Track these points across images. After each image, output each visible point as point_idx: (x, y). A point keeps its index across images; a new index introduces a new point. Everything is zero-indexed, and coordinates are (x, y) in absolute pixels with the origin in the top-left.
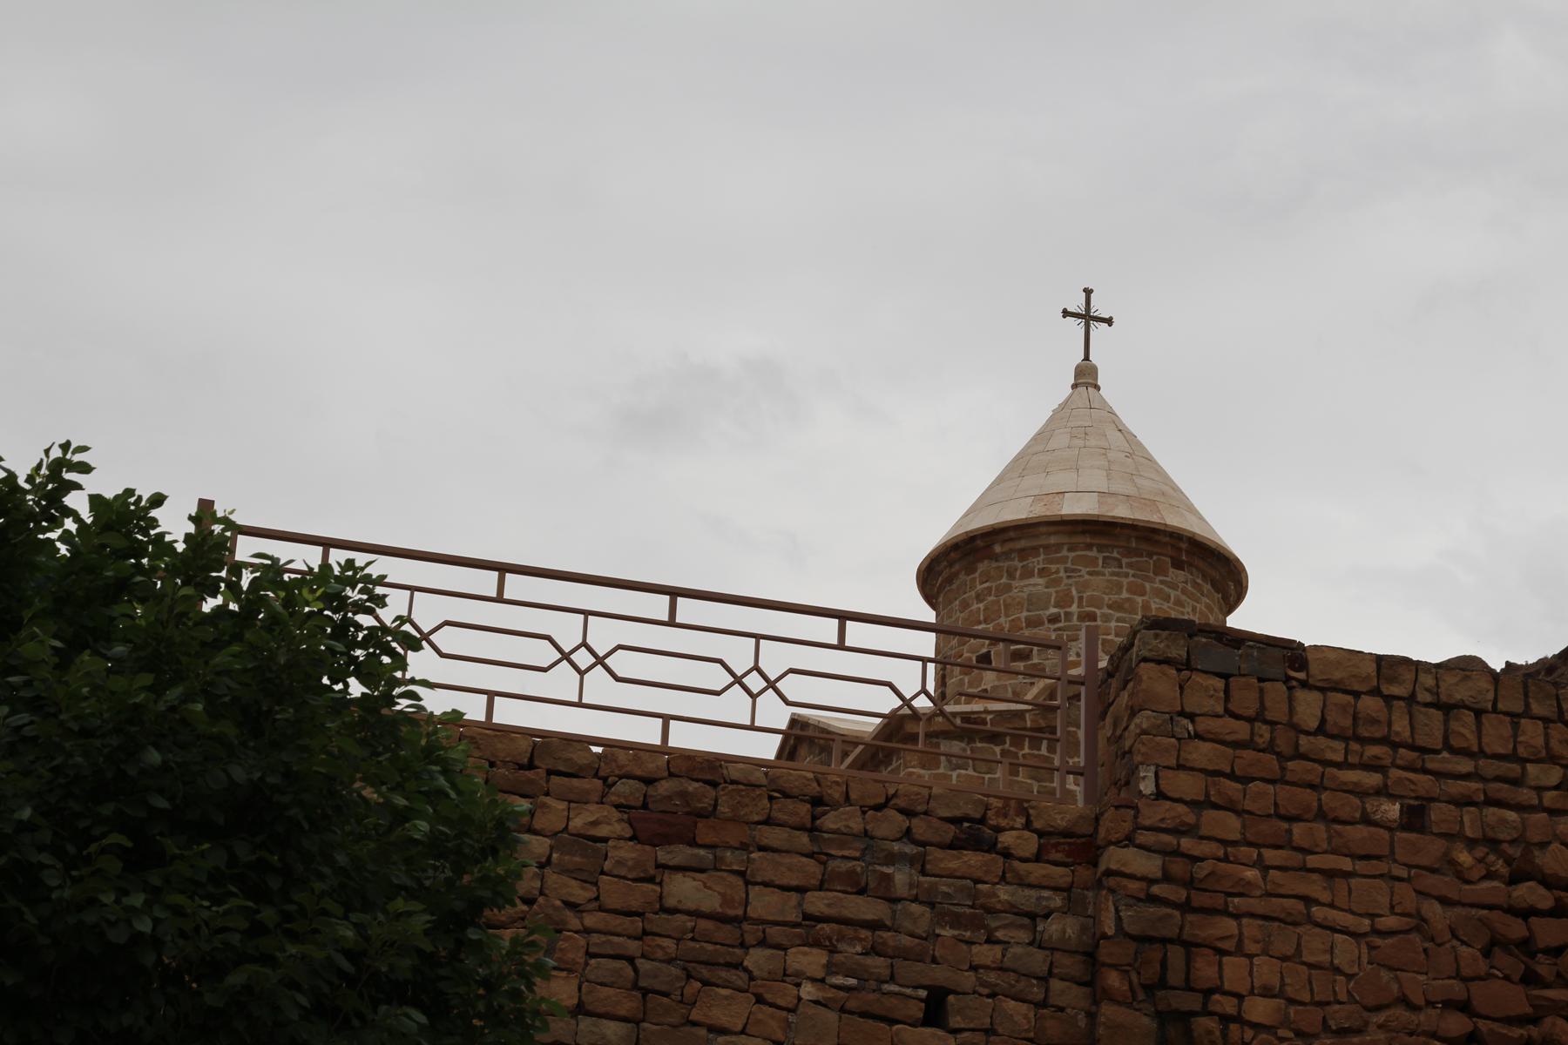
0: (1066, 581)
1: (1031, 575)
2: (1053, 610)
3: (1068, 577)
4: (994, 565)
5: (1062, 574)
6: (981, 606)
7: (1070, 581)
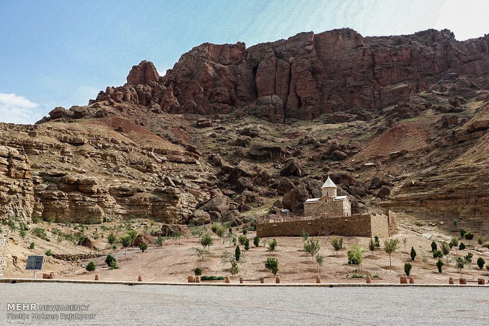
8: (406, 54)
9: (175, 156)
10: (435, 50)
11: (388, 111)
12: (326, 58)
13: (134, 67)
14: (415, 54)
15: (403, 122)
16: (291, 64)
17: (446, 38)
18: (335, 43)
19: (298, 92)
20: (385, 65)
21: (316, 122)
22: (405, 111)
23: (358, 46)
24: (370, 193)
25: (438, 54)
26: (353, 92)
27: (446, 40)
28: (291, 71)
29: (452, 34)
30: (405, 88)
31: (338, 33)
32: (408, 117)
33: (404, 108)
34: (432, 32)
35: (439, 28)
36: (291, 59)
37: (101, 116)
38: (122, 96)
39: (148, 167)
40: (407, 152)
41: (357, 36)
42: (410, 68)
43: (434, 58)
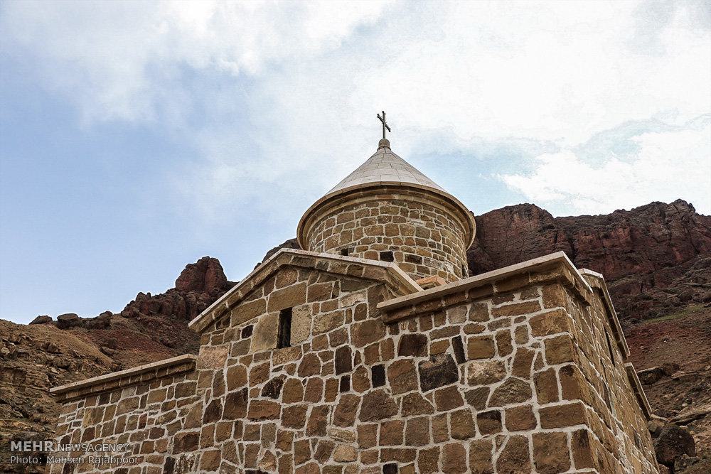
0: (436, 227)
1: (417, 217)
2: (430, 240)
3: (437, 226)
4: (391, 205)
5: (434, 222)
8: (623, 233)
12: (495, 250)
13: (189, 266)
14: (638, 234)
17: (682, 211)
18: (508, 226)
22: (644, 307)
23: (544, 228)
25: (676, 233)
27: (682, 214)
29: (691, 206)
30: (632, 283)
32: (652, 315)
33: (642, 302)
35: (668, 199)
40: (676, 368)
41: (543, 215)
42: (633, 255)
43: (670, 240)
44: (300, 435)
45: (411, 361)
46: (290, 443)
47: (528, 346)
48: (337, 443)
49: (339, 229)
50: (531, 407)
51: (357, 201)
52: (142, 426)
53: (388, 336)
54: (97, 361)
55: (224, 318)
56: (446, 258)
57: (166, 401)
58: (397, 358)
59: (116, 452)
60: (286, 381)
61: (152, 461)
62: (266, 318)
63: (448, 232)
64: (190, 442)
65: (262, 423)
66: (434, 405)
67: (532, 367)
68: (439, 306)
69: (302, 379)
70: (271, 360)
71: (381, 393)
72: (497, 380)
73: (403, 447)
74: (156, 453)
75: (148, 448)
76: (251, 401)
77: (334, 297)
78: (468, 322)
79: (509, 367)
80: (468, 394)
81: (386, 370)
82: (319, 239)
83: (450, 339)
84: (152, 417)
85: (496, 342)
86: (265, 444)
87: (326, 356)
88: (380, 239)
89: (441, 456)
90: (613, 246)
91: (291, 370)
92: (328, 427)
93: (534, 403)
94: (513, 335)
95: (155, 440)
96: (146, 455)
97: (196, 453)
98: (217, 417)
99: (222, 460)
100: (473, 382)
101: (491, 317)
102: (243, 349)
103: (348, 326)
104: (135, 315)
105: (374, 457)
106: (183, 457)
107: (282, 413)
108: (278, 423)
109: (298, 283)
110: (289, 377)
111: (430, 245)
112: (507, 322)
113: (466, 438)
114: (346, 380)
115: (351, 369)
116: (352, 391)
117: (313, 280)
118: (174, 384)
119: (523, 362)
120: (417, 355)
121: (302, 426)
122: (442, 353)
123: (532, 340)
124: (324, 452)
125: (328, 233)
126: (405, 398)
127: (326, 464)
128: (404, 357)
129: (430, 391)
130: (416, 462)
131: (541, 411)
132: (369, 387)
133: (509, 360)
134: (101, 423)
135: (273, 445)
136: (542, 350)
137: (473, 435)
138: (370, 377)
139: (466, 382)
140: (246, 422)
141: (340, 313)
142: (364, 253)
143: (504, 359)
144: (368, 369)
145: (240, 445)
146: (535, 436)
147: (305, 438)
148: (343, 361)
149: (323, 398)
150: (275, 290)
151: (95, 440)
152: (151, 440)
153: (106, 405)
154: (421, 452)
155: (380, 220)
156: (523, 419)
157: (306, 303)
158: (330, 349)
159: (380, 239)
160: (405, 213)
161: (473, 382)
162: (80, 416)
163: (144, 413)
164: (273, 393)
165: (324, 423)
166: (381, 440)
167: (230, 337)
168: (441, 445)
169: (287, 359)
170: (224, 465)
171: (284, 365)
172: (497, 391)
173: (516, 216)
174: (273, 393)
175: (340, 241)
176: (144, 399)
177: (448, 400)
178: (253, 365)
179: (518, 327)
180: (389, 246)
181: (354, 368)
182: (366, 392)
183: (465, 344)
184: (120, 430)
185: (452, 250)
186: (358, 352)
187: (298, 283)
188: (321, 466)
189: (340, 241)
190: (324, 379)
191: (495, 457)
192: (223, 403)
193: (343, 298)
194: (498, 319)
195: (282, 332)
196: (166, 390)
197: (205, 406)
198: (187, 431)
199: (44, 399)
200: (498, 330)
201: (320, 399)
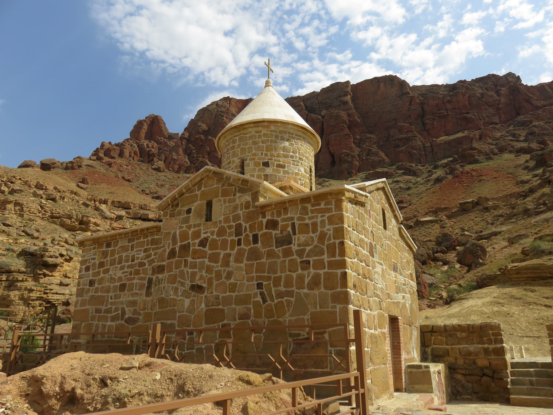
0: (295, 145)
2: (291, 154)
3: (296, 144)
5: (294, 142)
6: (264, 145)
7: (296, 146)
9: (142, 212)
10: (498, 95)
11: (443, 163)
15: (468, 168)
16: (323, 117)
17: (511, 82)
19: (331, 149)
20: (437, 113)
21: (351, 180)
24: (435, 260)
26: (398, 146)
28: (323, 125)
31: (378, 81)
32: (477, 162)
34: (492, 78)
35: (502, 72)
36: (323, 112)
37: (73, 168)
38: (118, 152)
39: (81, 222)
40: (487, 200)
41: (403, 84)
43: (499, 104)
44: (217, 267)
45: (271, 233)
46: (212, 271)
47: (325, 230)
48: (235, 272)
49: (239, 146)
50: (324, 259)
51: (250, 130)
52: (133, 260)
53: (260, 219)
54: (75, 193)
55: (176, 202)
56: (300, 164)
57: (146, 247)
58: (265, 231)
59: (119, 274)
60: (210, 239)
61: (141, 279)
62: (198, 204)
63: (303, 148)
64: (160, 269)
65: (198, 260)
66: (281, 255)
67: (326, 240)
68: (285, 206)
69: (218, 239)
70: (202, 228)
71: (256, 248)
72: (309, 245)
73: (266, 274)
74: (142, 275)
75: (137, 272)
76: (193, 249)
77: (234, 196)
78: (299, 215)
79: (316, 239)
80: (297, 251)
81: (259, 236)
82: (228, 150)
83: (290, 223)
84: (138, 256)
85: (311, 226)
86: (200, 271)
87: (230, 227)
88: (262, 154)
89: (283, 280)
90: (454, 109)
91: (212, 233)
92: (231, 264)
93: (325, 258)
94: (319, 224)
95: (141, 268)
96: (136, 277)
97: (164, 275)
98: (174, 256)
99: (178, 279)
100: (299, 245)
101: (310, 213)
102: (186, 221)
103: (241, 212)
104: (99, 159)
105: (252, 279)
106: (157, 277)
107: (208, 256)
108: (206, 260)
109: (215, 186)
110: (211, 237)
111: (291, 157)
112: (317, 216)
113: (294, 272)
114: (239, 240)
115: (242, 235)
116: (243, 246)
117: (223, 185)
118: (150, 238)
119: (322, 237)
120: (274, 230)
121: (218, 262)
122: (285, 230)
123: (327, 227)
124: (229, 275)
125: (233, 148)
126: (267, 251)
127: (230, 281)
128: (267, 231)
129: (279, 248)
130: (271, 282)
131: (328, 262)
132: (250, 244)
133: (316, 236)
134: (108, 259)
135: (204, 271)
136: (331, 232)
137: (297, 271)
138: (251, 239)
139: (296, 245)
140: (190, 259)
141: (237, 205)
142: (253, 162)
143: (314, 235)
144: (251, 235)
145: (187, 272)
146: (324, 273)
147: (220, 268)
148: (238, 232)
149: (229, 249)
150: (203, 189)
151: (105, 268)
152: (139, 268)
153: (110, 249)
154: (274, 277)
155: (263, 142)
156: (320, 264)
157: (220, 198)
158: (232, 223)
159: (262, 154)
160: (277, 137)
161: (299, 245)
162: (95, 254)
163: (133, 254)
164: (203, 245)
165: (229, 262)
166: (256, 271)
167: (179, 214)
168: (283, 275)
169: (210, 228)
170: (179, 282)
171: (209, 230)
172: (309, 250)
173: (382, 85)
174: (203, 245)
175: (239, 154)
176: (132, 246)
177: (288, 252)
178: (192, 230)
179: (321, 220)
180: (267, 158)
181: (244, 234)
182: (249, 247)
183: (297, 226)
184: (120, 263)
185: (304, 158)
186: (246, 227)
187: (215, 186)
188: (228, 283)
189: (239, 154)
190: (229, 239)
191: (306, 282)
192: (177, 249)
193: (239, 197)
194: (313, 215)
195: (207, 212)
196: (145, 241)
197: (168, 251)
198: (159, 264)
199: (39, 222)
200: (313, 220)
201: (227, 249)
